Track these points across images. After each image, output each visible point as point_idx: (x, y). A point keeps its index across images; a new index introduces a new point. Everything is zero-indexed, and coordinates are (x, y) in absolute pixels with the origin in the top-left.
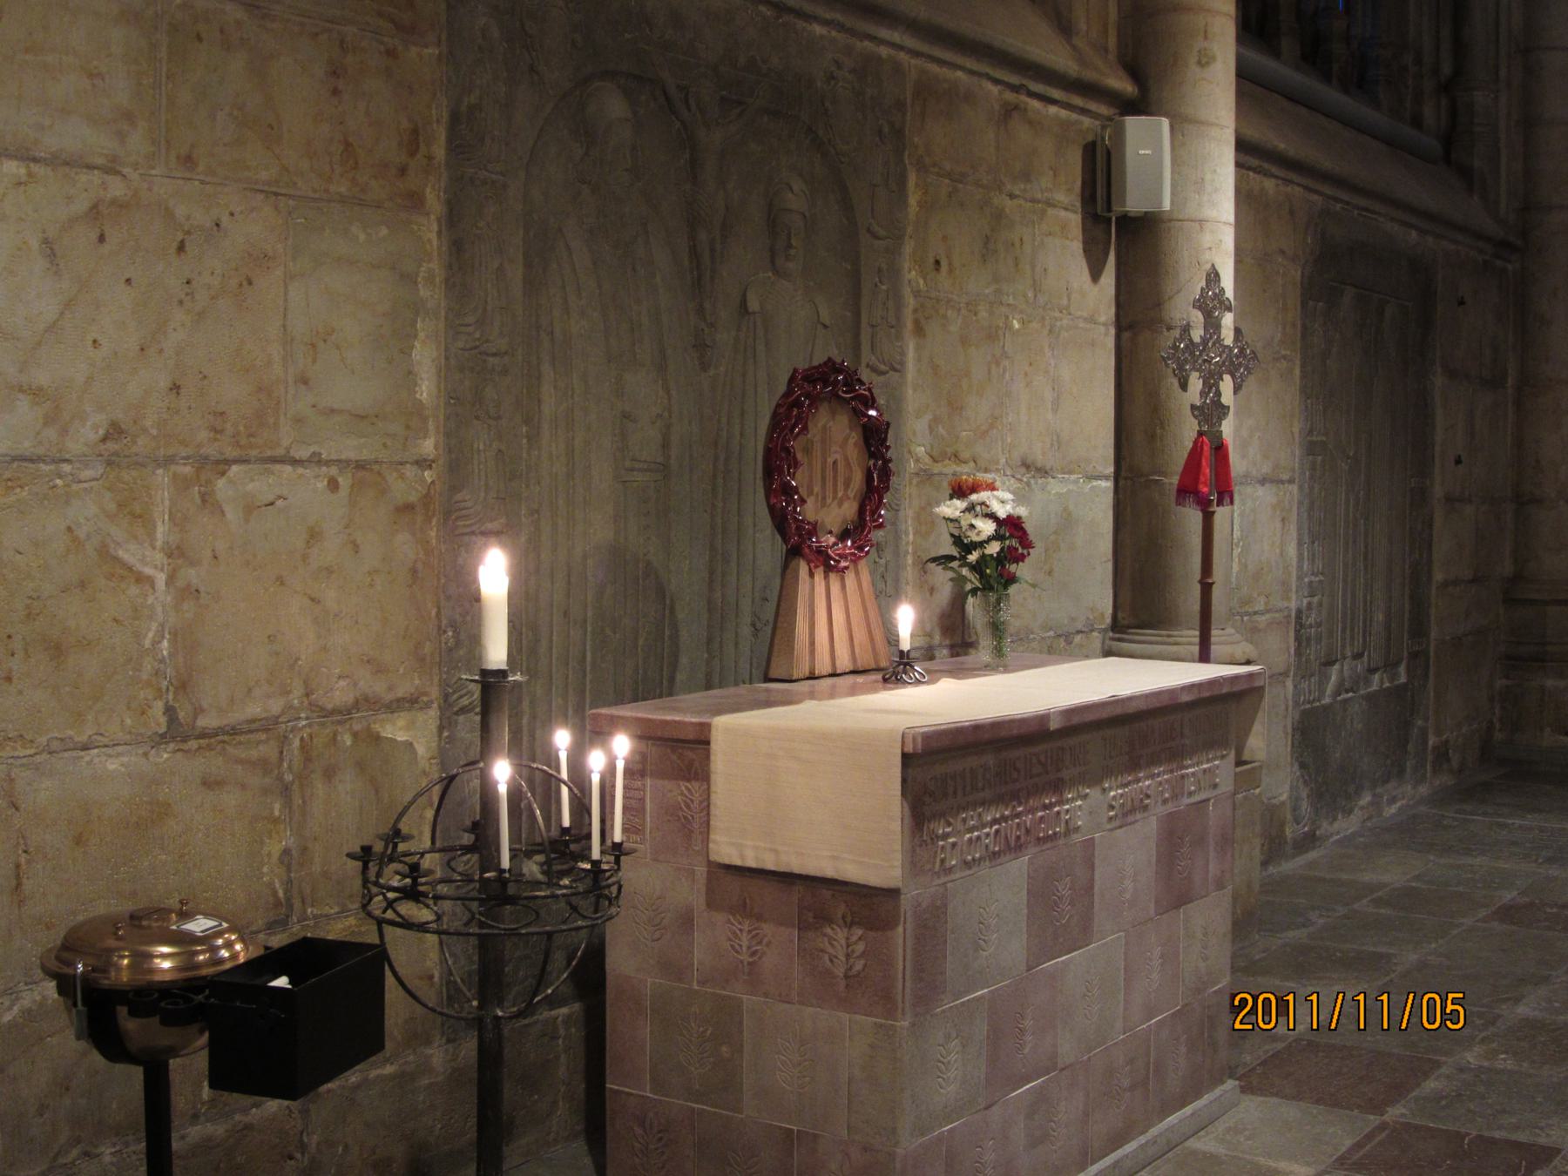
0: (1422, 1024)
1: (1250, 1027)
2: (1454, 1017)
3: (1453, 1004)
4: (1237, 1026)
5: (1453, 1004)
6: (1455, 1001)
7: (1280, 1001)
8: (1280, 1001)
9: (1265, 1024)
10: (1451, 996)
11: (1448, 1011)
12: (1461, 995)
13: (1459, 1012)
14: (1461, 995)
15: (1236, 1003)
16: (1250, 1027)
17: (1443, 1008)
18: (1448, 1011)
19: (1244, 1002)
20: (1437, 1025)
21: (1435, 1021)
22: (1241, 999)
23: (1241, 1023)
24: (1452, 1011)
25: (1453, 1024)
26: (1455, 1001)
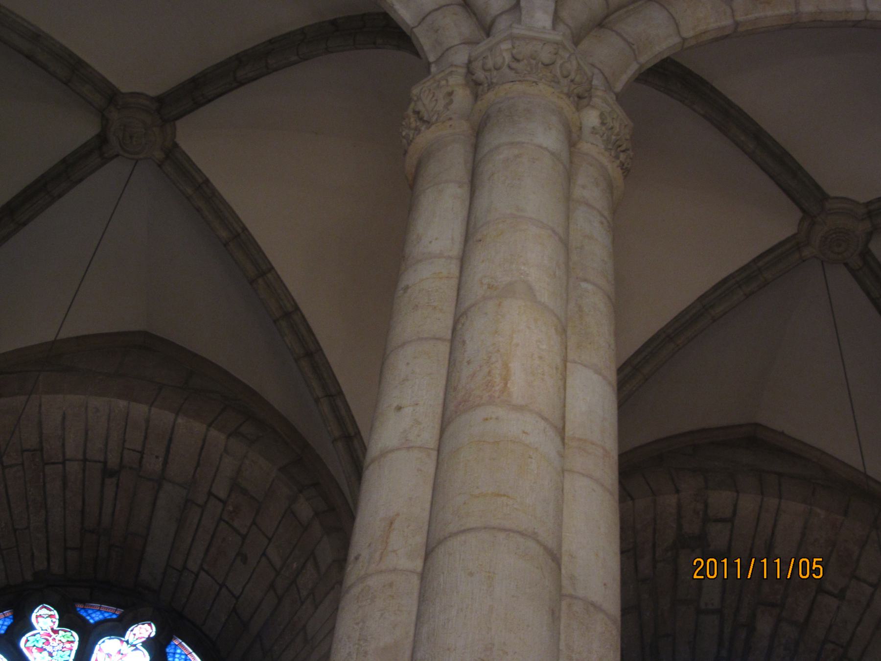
0: (799, 576)
1: (702, 577)
2: (817, 571)
3: (816, 564)
4: (695, 577)
5: (816, 564)
6: (817, 563)
7: (719, 562)
8: (719, 562)
9: (711, 575)
10: (815, 560)
11: (814, 568)
12: (821, 559)
13: (819, 569)
14: (821, 559)
15: (695, 564)
16: (702, 577)
17: (811, 566)
18: (814, 568)
19: (699, 563)
20: (807, 576)
21: (806, 574)
22: (697, 561)
23: (697, 575)
24: (816, 568)
25: (817, 575)
26: (817, 563)
